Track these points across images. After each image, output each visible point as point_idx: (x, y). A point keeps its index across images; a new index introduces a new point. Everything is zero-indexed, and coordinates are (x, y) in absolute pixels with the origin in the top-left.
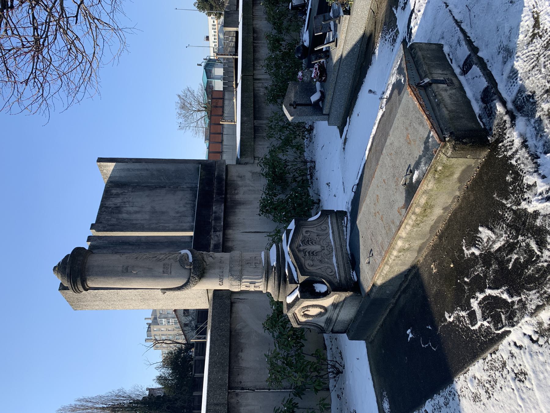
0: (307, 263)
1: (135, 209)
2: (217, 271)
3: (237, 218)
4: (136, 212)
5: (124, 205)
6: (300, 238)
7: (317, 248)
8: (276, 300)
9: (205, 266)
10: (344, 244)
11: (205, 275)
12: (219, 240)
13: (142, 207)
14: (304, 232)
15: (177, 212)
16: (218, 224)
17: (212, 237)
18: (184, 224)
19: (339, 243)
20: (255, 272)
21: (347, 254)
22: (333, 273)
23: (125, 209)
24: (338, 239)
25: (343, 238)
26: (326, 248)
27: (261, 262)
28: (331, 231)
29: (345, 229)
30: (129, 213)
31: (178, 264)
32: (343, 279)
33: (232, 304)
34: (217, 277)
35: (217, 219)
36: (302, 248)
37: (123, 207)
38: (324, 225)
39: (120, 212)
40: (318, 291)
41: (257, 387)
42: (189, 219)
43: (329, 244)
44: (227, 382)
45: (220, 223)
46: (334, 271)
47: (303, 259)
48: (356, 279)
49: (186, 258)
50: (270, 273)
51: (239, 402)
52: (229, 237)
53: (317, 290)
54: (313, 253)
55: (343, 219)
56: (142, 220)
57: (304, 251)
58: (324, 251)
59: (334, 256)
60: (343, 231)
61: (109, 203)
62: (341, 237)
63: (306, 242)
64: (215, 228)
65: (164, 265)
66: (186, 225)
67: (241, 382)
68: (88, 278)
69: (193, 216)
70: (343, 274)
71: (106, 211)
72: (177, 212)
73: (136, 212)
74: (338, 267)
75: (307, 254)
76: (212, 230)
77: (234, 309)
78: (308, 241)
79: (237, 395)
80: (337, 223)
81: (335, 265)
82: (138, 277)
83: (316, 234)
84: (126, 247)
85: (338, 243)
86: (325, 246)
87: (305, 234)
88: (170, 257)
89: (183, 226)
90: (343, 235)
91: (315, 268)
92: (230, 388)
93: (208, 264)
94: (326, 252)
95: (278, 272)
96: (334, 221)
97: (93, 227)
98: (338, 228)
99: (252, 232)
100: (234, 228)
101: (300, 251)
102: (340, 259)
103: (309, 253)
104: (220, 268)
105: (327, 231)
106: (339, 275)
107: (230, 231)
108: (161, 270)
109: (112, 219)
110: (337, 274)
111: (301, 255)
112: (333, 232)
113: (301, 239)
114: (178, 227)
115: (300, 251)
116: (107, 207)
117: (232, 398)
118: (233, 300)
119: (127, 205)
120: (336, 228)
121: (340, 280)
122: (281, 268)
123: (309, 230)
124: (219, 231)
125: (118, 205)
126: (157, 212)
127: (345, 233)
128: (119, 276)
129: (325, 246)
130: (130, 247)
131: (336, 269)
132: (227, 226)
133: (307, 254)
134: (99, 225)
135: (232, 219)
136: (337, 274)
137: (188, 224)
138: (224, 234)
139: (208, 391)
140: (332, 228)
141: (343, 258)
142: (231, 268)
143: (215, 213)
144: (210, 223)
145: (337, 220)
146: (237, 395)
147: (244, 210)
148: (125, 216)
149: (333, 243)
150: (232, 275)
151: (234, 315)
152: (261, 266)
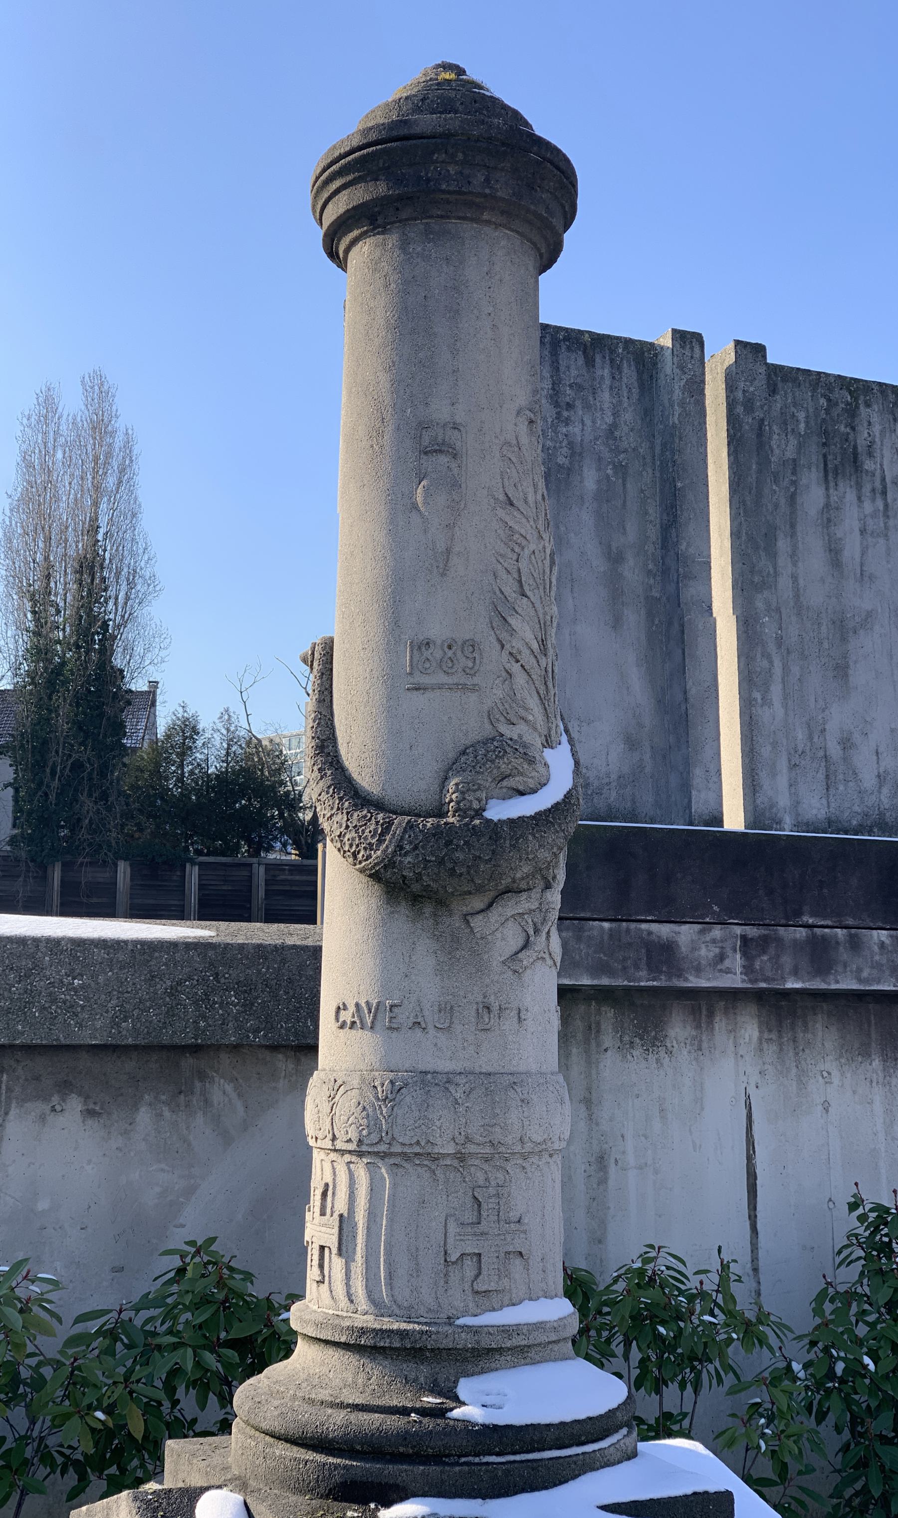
1: (852, 548)
2: (429, 988)
3: (830, 1065)
4: (834, 552)
5: (867, 489)
9: (460, 907)
11: (403, 909)
12: (698, 970)
13: (864, 577)
15: (846, 743)
16: (787, 960)
17: (717, 932)
18: (783, 781)
23: (851, 496)
27: (486, 1299)
30: (829, 515)
31: (475, 729)
35: (820, 956)
37: (859, 486)
39: (830, 474)
42: (815, 807)
45: (795, 973)
50: (409, 1368)
52: (720, 1023)
56: (795, 578)
61: (875, 419)
64: (764, 943)
66: (779, 791)
69: (831, 824)
71: (836, 412)
72: (846, 743)
73: (834, 552)
76: (752, 932)
84: (654, 511)
88: (520, 679)
89: (774, 774)
93: (477, 922)
95: (404, 1436)
97: (750, 352)
99: (750, 1158)
100: (771, 1050)
104: (447, 1010)
107: (750, 1029)
109: (793, 441)
114: (766, 751)
116: (852, 412)
119: (868, 507)
122: (437, 1459)
124: (748, 969)
125: (868, 465)
126: (844, 639)
130: (653, 532)
132: (782, 1010)
134: (761, 381)
135: (824, 1036)
137: (784, 801)
138: (732, 996)
142: (447, 1080)
143: (855, 944)
144: (792, 917)
147: (878, 1107)
148: (813, 496)
150: (396, 1090)
152: (457, 1297)
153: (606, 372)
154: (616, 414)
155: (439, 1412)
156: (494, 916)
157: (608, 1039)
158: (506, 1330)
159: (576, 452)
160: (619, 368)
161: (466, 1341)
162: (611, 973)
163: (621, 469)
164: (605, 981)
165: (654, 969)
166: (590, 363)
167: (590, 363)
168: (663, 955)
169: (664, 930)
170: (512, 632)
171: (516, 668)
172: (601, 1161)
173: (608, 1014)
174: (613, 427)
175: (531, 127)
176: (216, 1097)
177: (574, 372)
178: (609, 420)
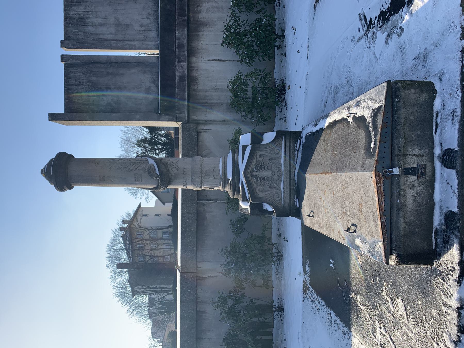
1: (100, 20)
3: (200, 43)
4: (102, 25)
5: (87, 16)
6: (254, 162)
7: (267, 173)
12: (184, 72)
13: (106, 18)
14: (258, 156)
15: (142, 26)
16: (182, 53)
17: (177, 67)
18: (150, 43)
19: (288, 168)
21: (294, 180)
22: (279, 198)
23: (89, 20)
26: (276, 173)
27: (219, 174)
28: (283, 155)
29: (296, 153)
30: (94, 26)
32: (287, 205)
33: (198, 133)
34: (181, 185)
35: (181, 46)
36: (254, 173)
37: (87, 18)
39: (85, 25)
42: (153, 34)
43: (280, 170)
45: (184, 52)
46: (280, 196)
47: (255, 184)
48: (298, 207)
52: (193, 65)
53: (265, 208)
54: (263, 179)
56: (108, 34)
57: (257, 177)
58: (274, 177)
59: (282, 182)
61: (72, 13)
63: (260, 167)
64: (179, 58)
66: (152, 43)
67: (206, 196)
69: (157, 31)
70: (287, 201)
71: (72, 23)
72: (142, 26)
73: (102, 25)
74: (285, 194)
75: (259, 179)
76: (177, 61)
77: (200, 138)
78: (261, 166)
79: (204, 204)
80: (290, 146)
81: (282, 190)
83: (269, 158)
84: (98, 65)
85: (288, 168)
87: (259, 159)
88: (139, 168)
89: (148, 45)
92: (198, 200)
93: (173, 174)
94: (275, 177)
95: (233, 187)
96: (288, 144)
97: (63, 44)
98: (290, 152)
99: (216, 61)
100: (198, 55)
102: (288, 185)
103: (260, 178)
104: (184, 178)
106: (284, 201)
107: (194, 59)
109: (79, 33)
111: (253, 180)
113: (254, 163)
114: (144, 46)
115: (252, 176)
116: (71, 18)
118: (199, 130)
119: (91, 16)
122: (235, 183)
123: (263, 153)
124: (184, 62)
125: (82, 15)
126: (121, 25)
128: (98, 183)
130: (103, 66)
132: (191, 52)
133: (259, 179)
134: (68, 42)
135: (195, 44)
137: (153, 43)
138: (189, 63)
142: (192, 178)
143: (179, 39)
144: (174, 52)
145: (290, 143)
147: (207, 33)
148: (90, 29)
150: (194, 184)
151: (200, 144)
153: (72, 74)
154: (80, 73)
155: (231, 182)
156: (172, 172)
157: (196, 87)
158: (222, 172)
159: (89, 81)
160: (70, 71)
161: (223, 177)
162: (185, 89)
163: (91, 72)
164: (186, 90)
165: (184, 80)
166: (70, 78)
167: (70, 78)
168: (181, 78)
169: (177, 78)
170: (132, 170)
171: (138, 169)
172: (215, 89)
173: (191, 87)
174: (82, 73)
175: (52, 160)
176: (205, 154)
177: (73, 81)
178: (81, 74)
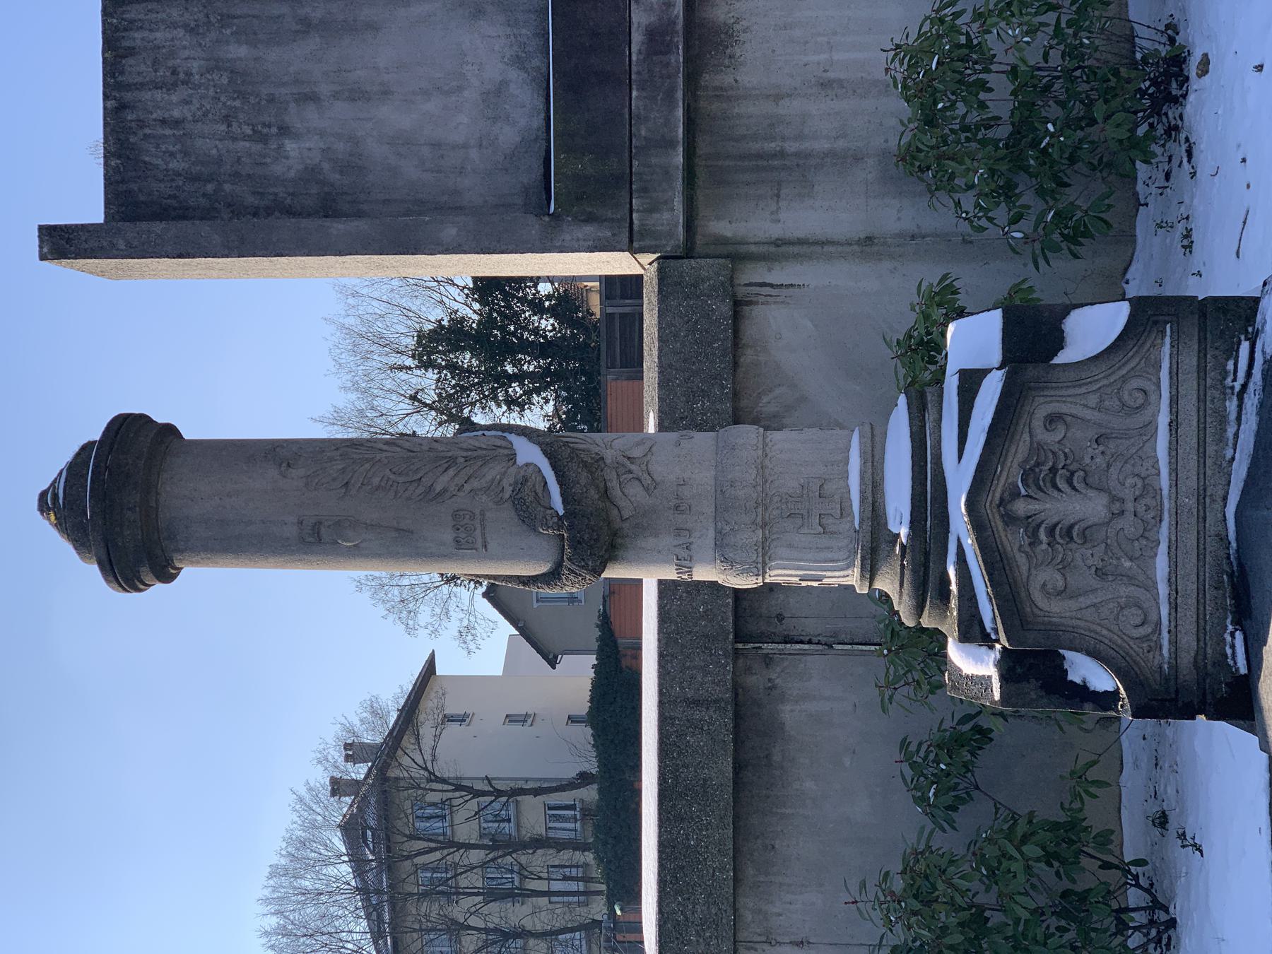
0: (1040, 580)
2: (667, 541)
6: (1019, 452)
7: (1085, 507)
8: (909, 622)
9: (617, 524)
10: (1215, 491)
11: (620, 553)
14: (1038, 423)
19: (1193, 483)
20: (820, 549)
21: (1223, 539)
22: (1147, 629)
24: (1193, 464)
25: (1219, 454)
26: (1129, 506)
27: (845, 511)
28: (1163, 419)
29: (1232, 406)
31: (508, 513)
32: (1186, 660)
33: (738, 306)
34: (667, 562)
36: (1021, 507)
38: (1135, 383)
40: (1078, 680)
41: (842, 637)
43: (1148, 488)
44: (730, 628)
46: (1154, 617)
47: (1021, 559)
48: (1243, 670)
49: (539, 490)
50: (882, 554)
51: (774, 687)
53: (1074, 677)
54: (1066, 533)
55: (1233, 352)
57: (1031, 525)
58: (1119, 523)
59: (1163, 548)
60: (1223, 420)
62: (1211, 449)
63: (1047, 474)
65: (455, 515)
67: (780, 618)
68: (176, 556)
70: (1188, 641)
74: (1174, 607)
75: (1042, 535)
77: (750, 331)
78: (1053, 470)
79: (768, 660)
80: (1202, 371)
81: (1163, 589)
82: (366, 556)
83: (1092, 433)
85: (1190, 482)
86: (1128, 494)
87: (1042, 435)
88: (475, 484)
90: (1221, 439)
91: (1073, 604)
92: (739, 638)
93: (626, 514)
94: (1128, 525)
95: (914, 571)
96: (1190, 361)
98: (1202, 399)
101: (1010, 519)
102: (1189, 564)
103: (1051, 531)
104: (679, 531)
105: (1148, 412)
106: (1174, 643)
108: (448, 536)
110: (1165, 635)
111: (1012, 541)
112: (1174, 425)
113: (1020, 457)
115: (1010, 519)
117: (748, 670)
118: (741, 291)
120: (1189, 405)
121: (1175, 668)
122: (927, 554)
123: (1064, 408)
127: (1231, 431)
128: (292, 553)
129: (1128, 494)
131: (1164, 611)
133: (1042, 535)
136: (1165, 635)
139: (661, 655)
140: (1174, 401)
141: (1201, 556)
142: (719, 532)
145: (1202, 353)
146: (768, 660)
149: (1165, 481)
150: (725, 560)
151: (747, 357)
152: (844, 526)
153: (137, 35)
154: (174, 26)
155: (903, 547)
156: (622, 503)
157: (728, 79)
158: (863, 500)
159: (216, 65)
160: (132, 22)
161: (867, 526)
163: (225, 20)
164: (680, 94)
165: (668, 49)
166: (131, 52)
167: (131, 52)
168: (657, 38)
169: (637, 38)
170: (445, 490)
171: (467, 487)
172: (825, 85)
173: (706, 79)
174: (186, 26)
176: (772, 409)
177: (143, 68)
178: (180, 33)
